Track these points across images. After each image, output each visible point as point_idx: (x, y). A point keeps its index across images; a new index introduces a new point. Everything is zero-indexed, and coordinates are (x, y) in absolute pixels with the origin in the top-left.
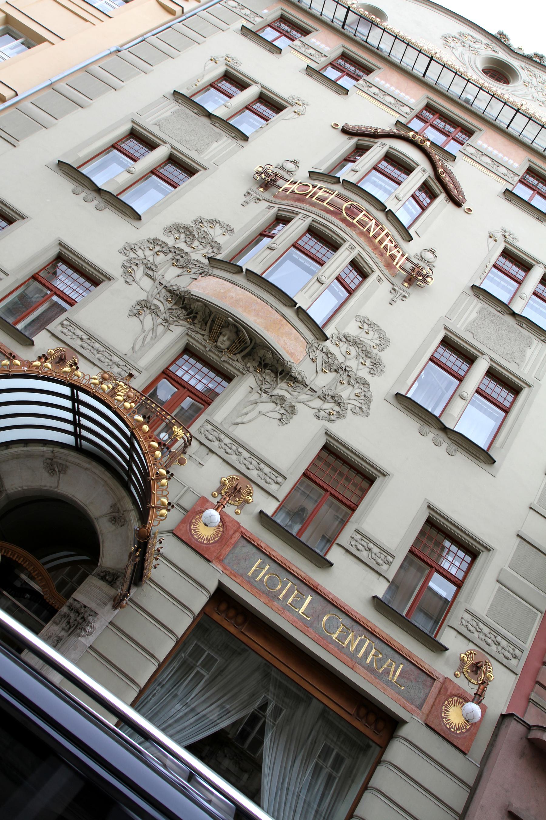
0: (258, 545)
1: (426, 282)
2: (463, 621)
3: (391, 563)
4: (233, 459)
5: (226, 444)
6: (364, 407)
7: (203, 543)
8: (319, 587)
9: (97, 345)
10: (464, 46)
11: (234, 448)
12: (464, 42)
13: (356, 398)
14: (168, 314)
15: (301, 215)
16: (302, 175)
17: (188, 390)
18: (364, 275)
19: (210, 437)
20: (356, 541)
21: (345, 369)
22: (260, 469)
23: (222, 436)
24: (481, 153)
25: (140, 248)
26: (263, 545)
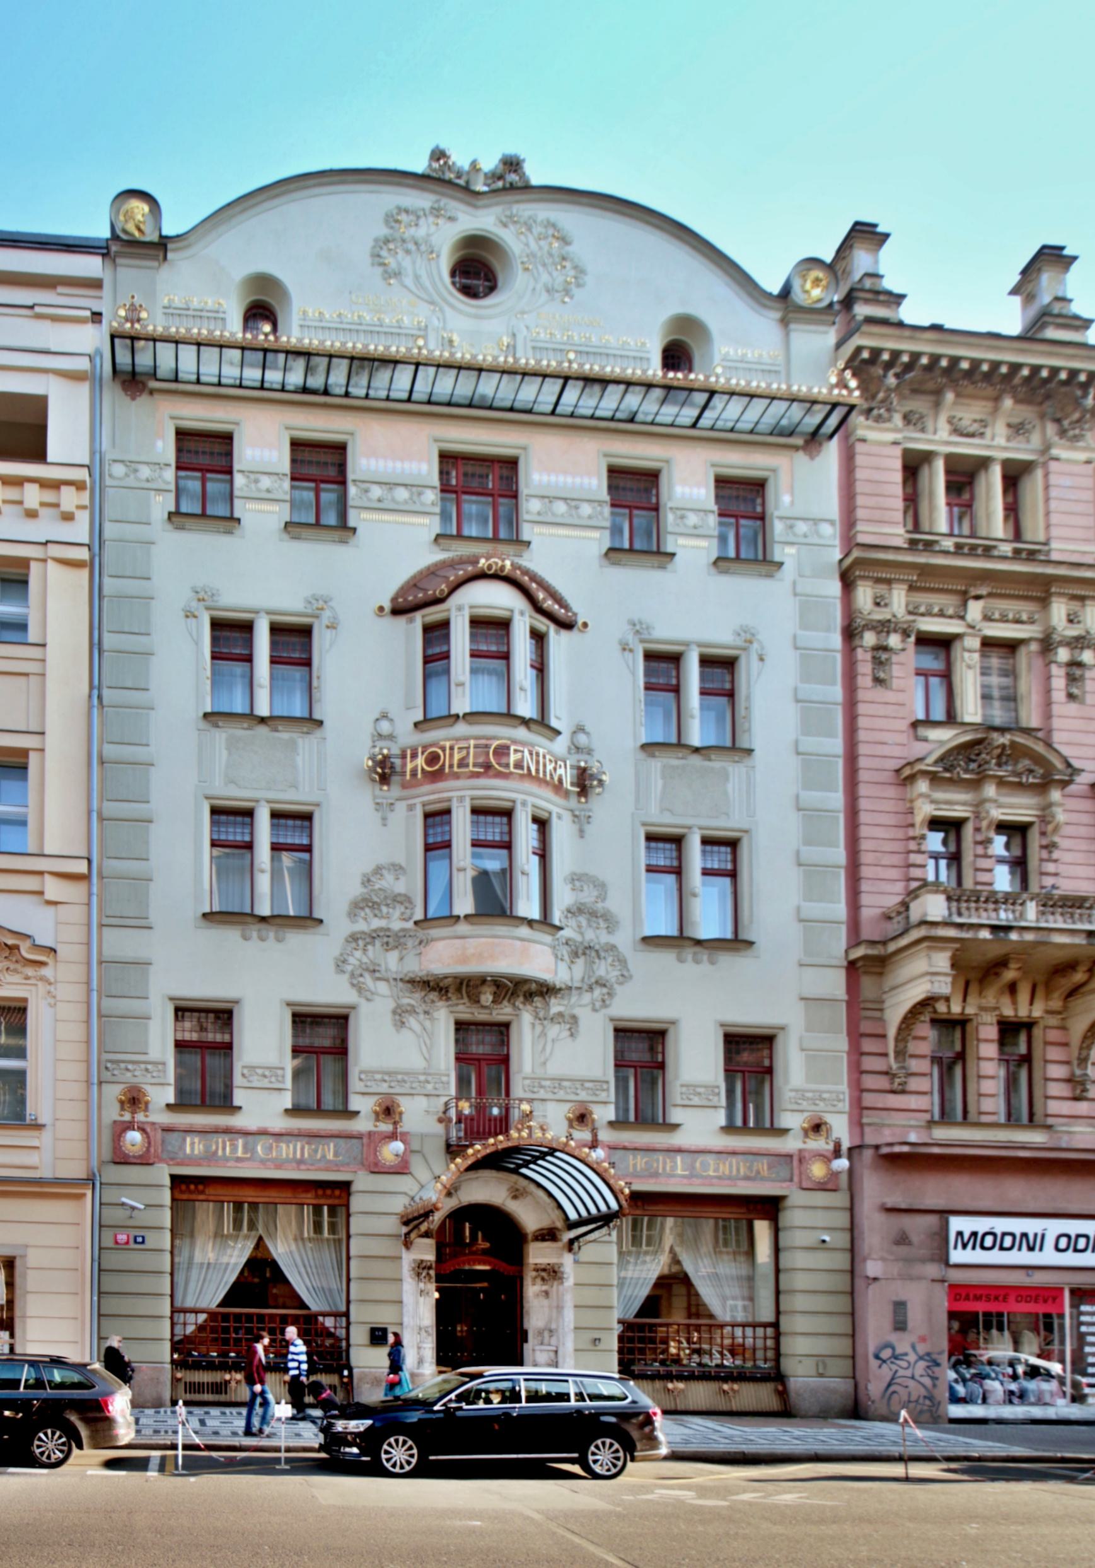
4: (561, 1095)
6: (626, 973)
26: (626, 1144)
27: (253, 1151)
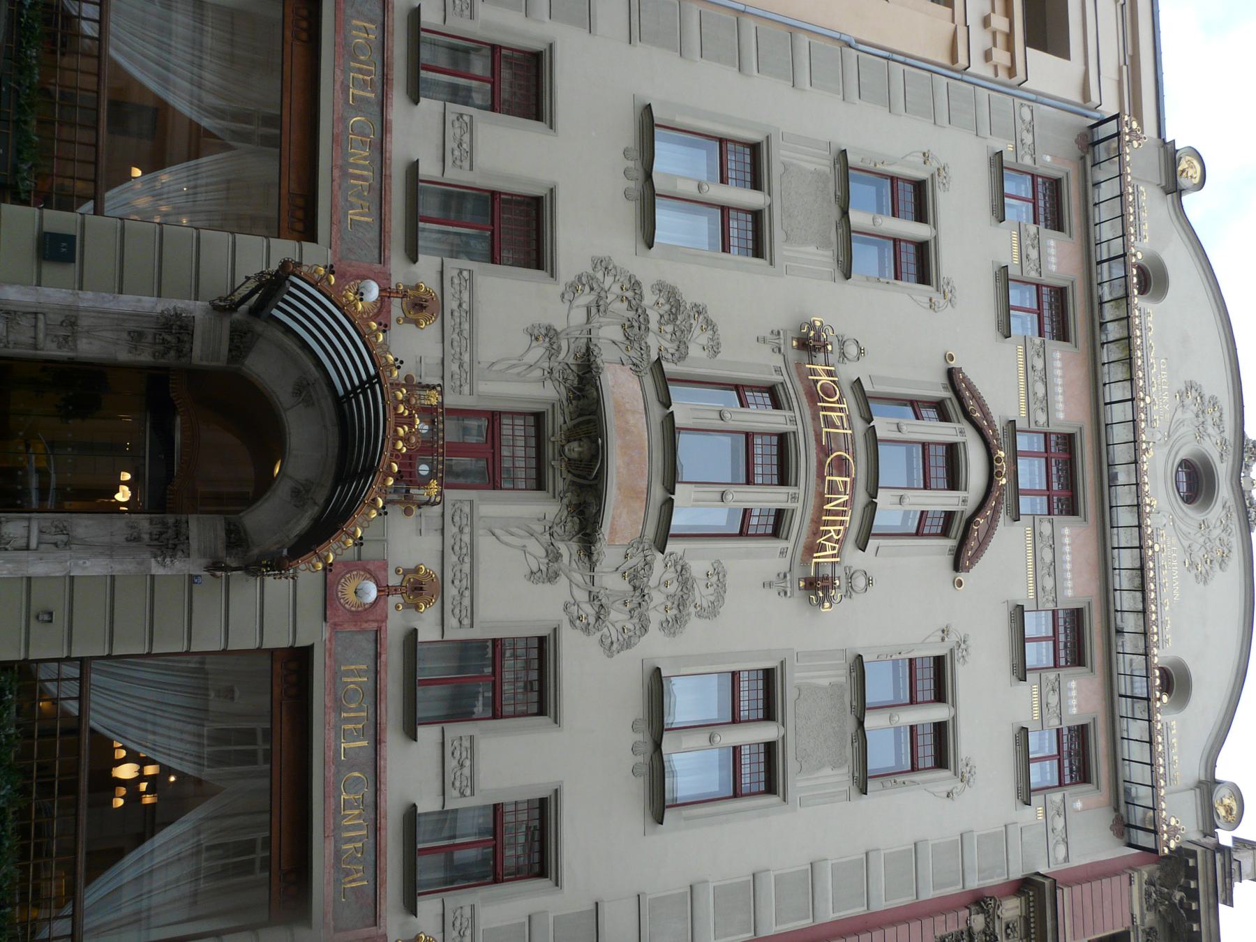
0: (380, 654)
1: (821, 603)
2: (459, 912)
3: (465, 796)
4: (451, 559)
5: (461, 540)
6: (615, 646)
7: (339, 599)
8: (382, 744)
9: (466, 326)
10: (1197, 416)
11: (464, 551)
12: (1203, 412)
13: (621, 630)
14: (560, 367)
15: (793, 414)
16: (848, 372)
17: (493, 454)
18: (775, 534)
19: (457, 519)
20: (461, 745)
21: (644, 596)
22: (462, 595)
23: (467, 530)
24: (1051, 543)
25: (615, 276)
26: (383, 657)
27: (358, 110)
